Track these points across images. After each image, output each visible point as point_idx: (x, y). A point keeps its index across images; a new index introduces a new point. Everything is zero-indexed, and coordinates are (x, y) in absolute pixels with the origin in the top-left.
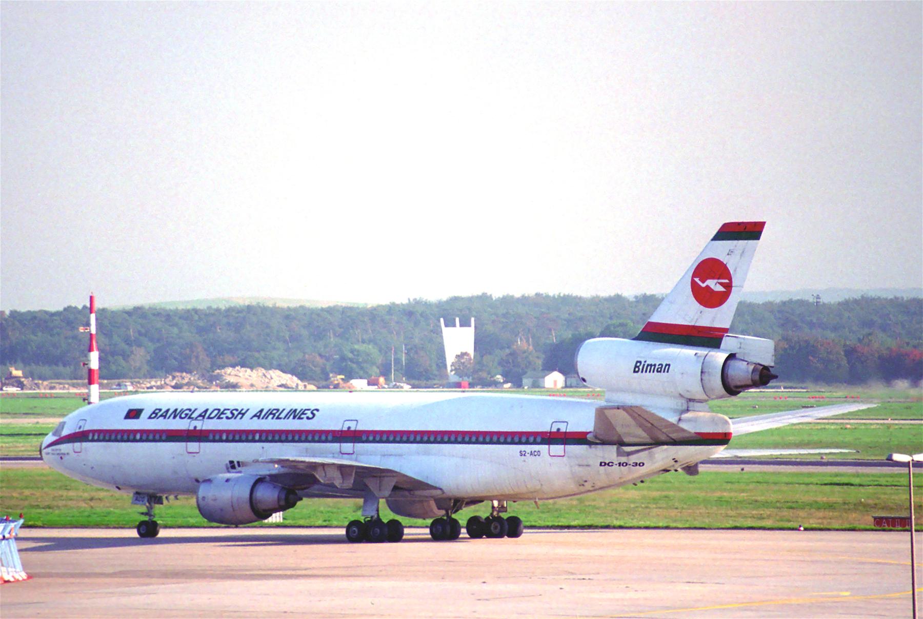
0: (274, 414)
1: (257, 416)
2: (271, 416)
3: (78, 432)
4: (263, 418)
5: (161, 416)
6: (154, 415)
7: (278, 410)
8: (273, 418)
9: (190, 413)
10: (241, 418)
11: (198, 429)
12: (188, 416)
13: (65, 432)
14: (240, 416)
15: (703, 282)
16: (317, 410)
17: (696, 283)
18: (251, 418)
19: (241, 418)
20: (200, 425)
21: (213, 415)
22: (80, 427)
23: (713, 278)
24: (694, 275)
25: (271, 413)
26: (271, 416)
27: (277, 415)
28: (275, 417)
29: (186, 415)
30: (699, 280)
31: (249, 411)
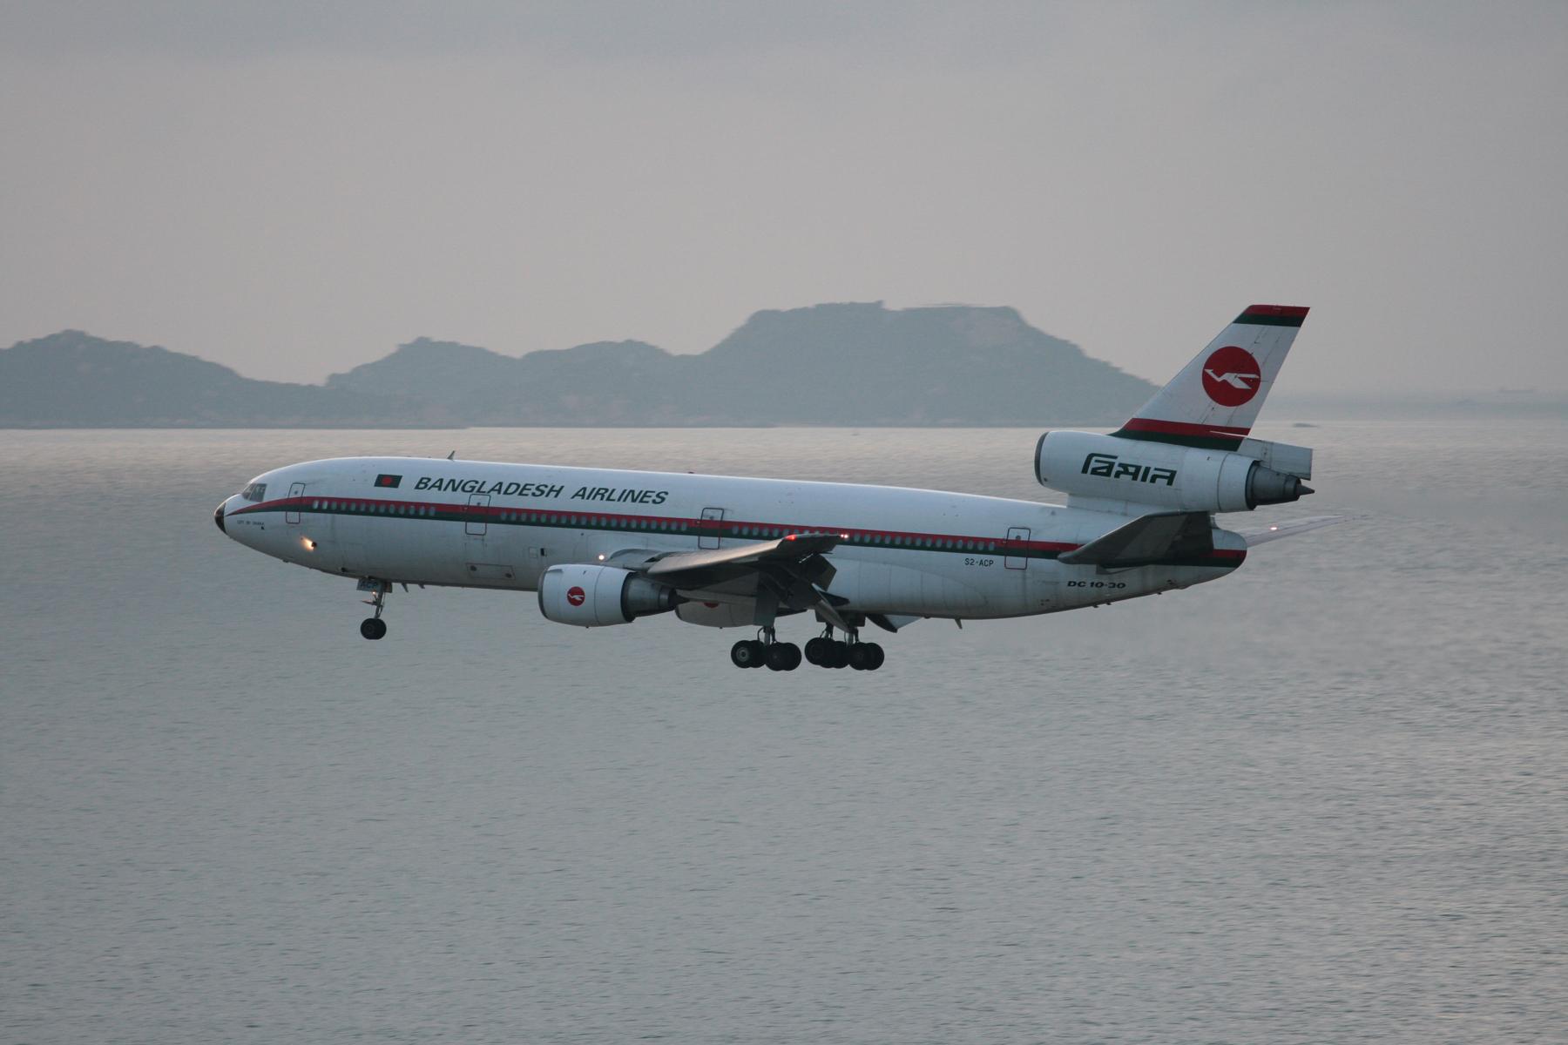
0: (603, 495)
2: (599, 497)
3: (293, 499)
4: (588, 498)
5: (433, 486)
6: (422, 486)
7: (607, 490)
8: (602, 499)
9: (478, 486)
10: (556, 496)
11: (481, 505)
12: (476, 489)
13: (267, 498)
14: (553, 494)
15: (1219, 376)
16: (666, 493)
17: (1210, 376)
18: (573, 497)
19: (556, 496)
20: (498, 501)
21: (510, 491)
22: (296, 493)
23: (1233, 370)
24: (1207, 366)
25: (597, 493)
26: (599, 497)
27: (606, 495)
28: (605, 499)
29: (473, 488)
30: (1213, 372)
31: (564, 489)
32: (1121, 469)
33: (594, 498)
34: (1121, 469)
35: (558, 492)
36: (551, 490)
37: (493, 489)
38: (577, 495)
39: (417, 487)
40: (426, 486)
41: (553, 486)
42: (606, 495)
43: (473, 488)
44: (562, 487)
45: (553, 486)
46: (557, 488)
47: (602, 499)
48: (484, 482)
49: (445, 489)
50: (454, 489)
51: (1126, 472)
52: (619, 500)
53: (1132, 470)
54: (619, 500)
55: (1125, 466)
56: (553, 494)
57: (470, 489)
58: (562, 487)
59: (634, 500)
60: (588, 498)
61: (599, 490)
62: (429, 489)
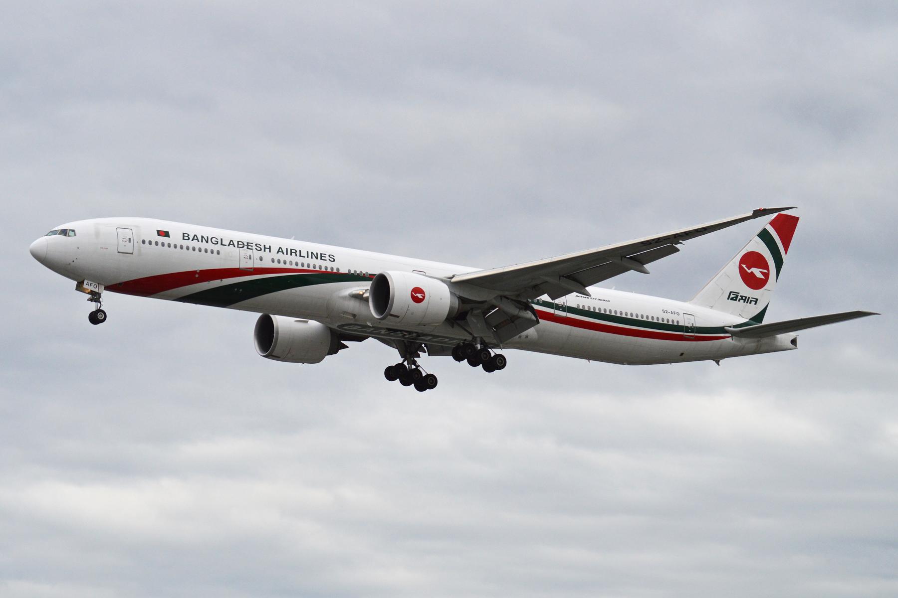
1: (280, 250)
4: (287, 254)
8: (296, 255)
14: (267, 250)
25: (291, 252)
27: (298, 253)
32: (740, 298)
33: (291, 255)
34: (740, 298)
39: (184, 239)
40: (189, 239)
41: (265, 246)
42: (298, 253)
43: (217, 242)
44: (270, 246)
45: (265, 246)
46: (267, 246)
47: (296, 255)
48: (222, 239)
49: (202, 242)
50: (207, 242)
51: (742, 299)
52: (308, 257)
53: (744, 298)
54: (308, 257)
55: (741, 296)
56: (267, 250)
57: (216, 242)
58: (270, 246)
59: (317, 258)
60: (287, 254)
61: (291, 250)
62: (192, 240)
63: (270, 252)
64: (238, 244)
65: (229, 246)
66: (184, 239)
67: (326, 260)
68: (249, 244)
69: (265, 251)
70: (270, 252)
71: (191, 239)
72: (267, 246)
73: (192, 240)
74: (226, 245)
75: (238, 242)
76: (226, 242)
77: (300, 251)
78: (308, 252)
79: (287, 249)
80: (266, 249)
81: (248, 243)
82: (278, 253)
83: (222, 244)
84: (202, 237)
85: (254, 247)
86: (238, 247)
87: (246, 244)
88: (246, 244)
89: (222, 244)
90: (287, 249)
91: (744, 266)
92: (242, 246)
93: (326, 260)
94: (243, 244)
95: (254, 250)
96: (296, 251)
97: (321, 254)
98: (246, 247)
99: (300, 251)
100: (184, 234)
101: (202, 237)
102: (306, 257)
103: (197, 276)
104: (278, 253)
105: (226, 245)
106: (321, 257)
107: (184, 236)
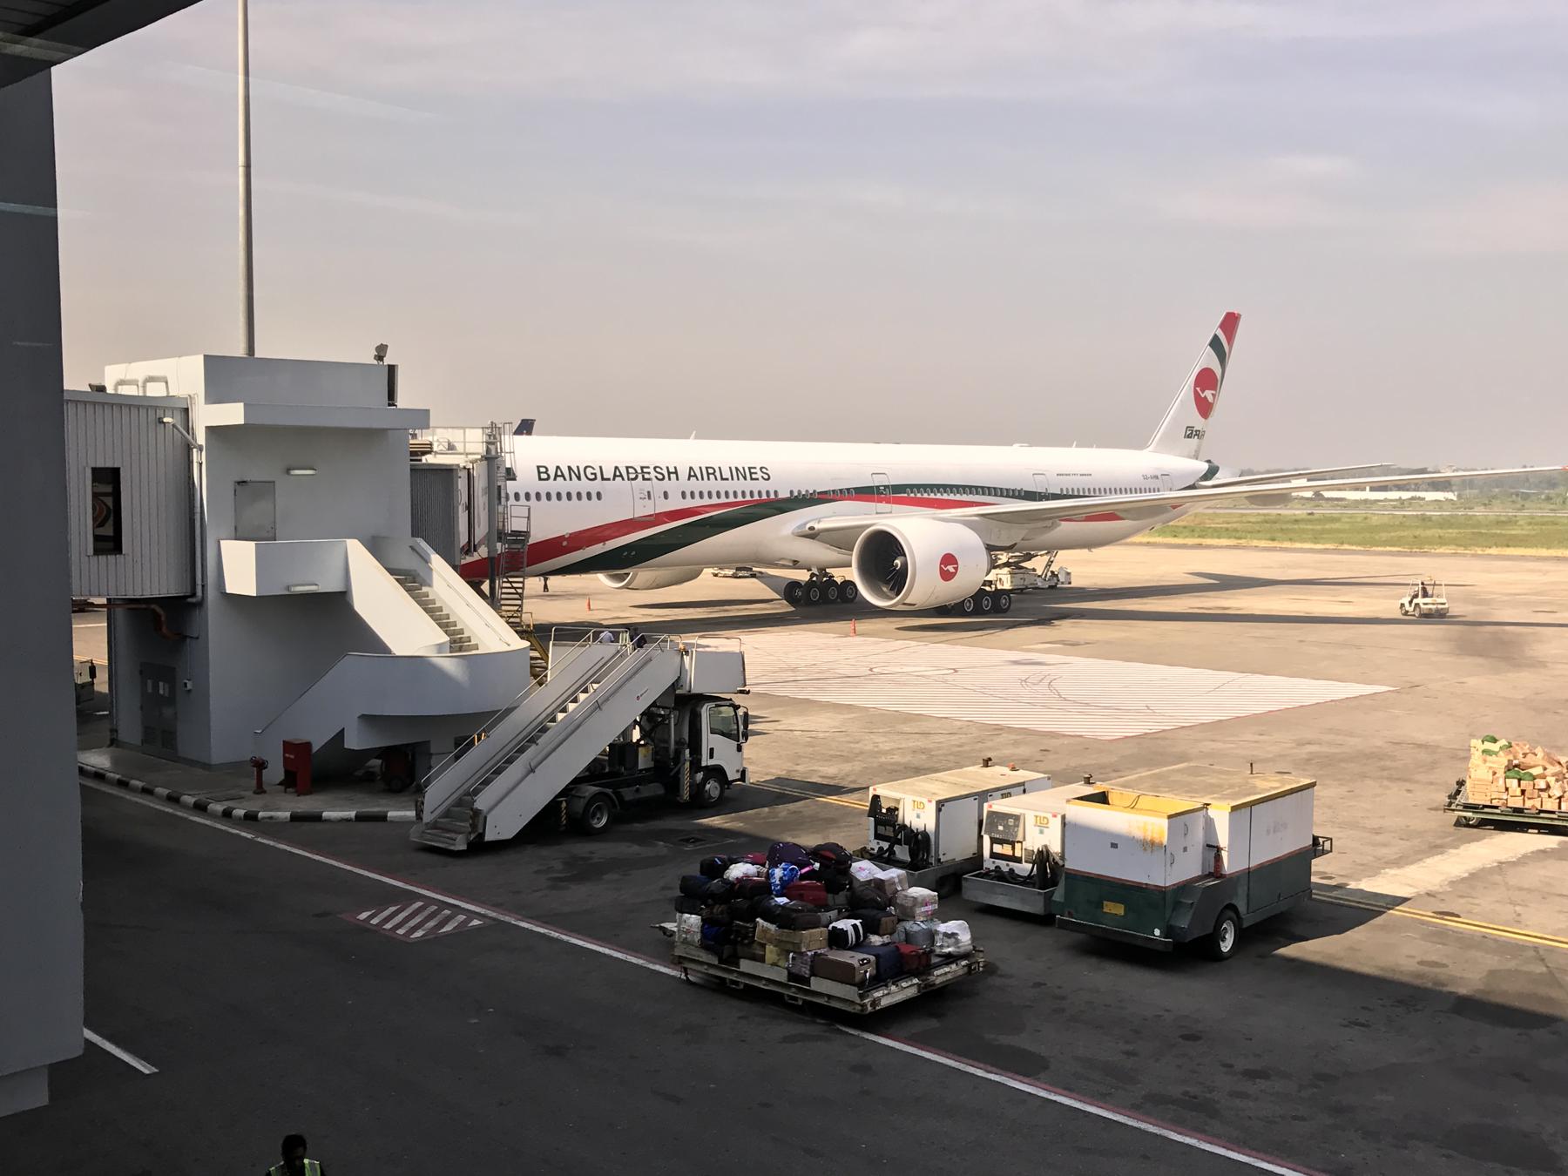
4: (703, 479)
5: (556, 476)
25: (708, 474)
35: (676, 473)
36: (669, 473)
37: (615, 476)
38: (690, 476)
39: (540, 479)
41: (667, 468)
43: (595, 474)
44: (675, 468)
45: (667, 468)
49: (571, 479)
50: (579, 478)
51: (1196, 435)
52: (732, 479)
55: (1196, 431)
56: (673, 476)
57: (593, 477)
58: (675, 468)
60: (703, 479)
62: (555, 479)
63: (677, 479)
64: (628, 473)
65: (614, 479)
66: (540, 479)
67: (757, 479)
68: (645, 470)
69: (670, 479)
70: (677, 479)
71: (552, 476)
72: (672, 470)
73: (555, 479)
74: (609, 479)
75: (627, 468)
76: (609, 473)
77: (720, 468)
78: (730, 468)
79: (700, 468)
80: (672, 475)
81: (642, 468)
82: (689, 479)
83: (603, 479)
84: (570, 468)
85: (653, 474)
86: (628, 479)
87: (639, 471)
88: (639, 471)
89: (603, 479)
90: (700, 468)
91: (1198, 389)
92: (633, 476)
93: (757, 479)
94: (636, 472)
95: (654, 479)
96: (715, 471)
97: (750, 468)
98: (640, 476)
99: (720, 468)
100: (538, 467)
101: (570, 468)
102: (730, 478)
103: (565, 544)
104: (689, 479)
105: (609, 479)
106: (751, 473)
107: (539, 473)
